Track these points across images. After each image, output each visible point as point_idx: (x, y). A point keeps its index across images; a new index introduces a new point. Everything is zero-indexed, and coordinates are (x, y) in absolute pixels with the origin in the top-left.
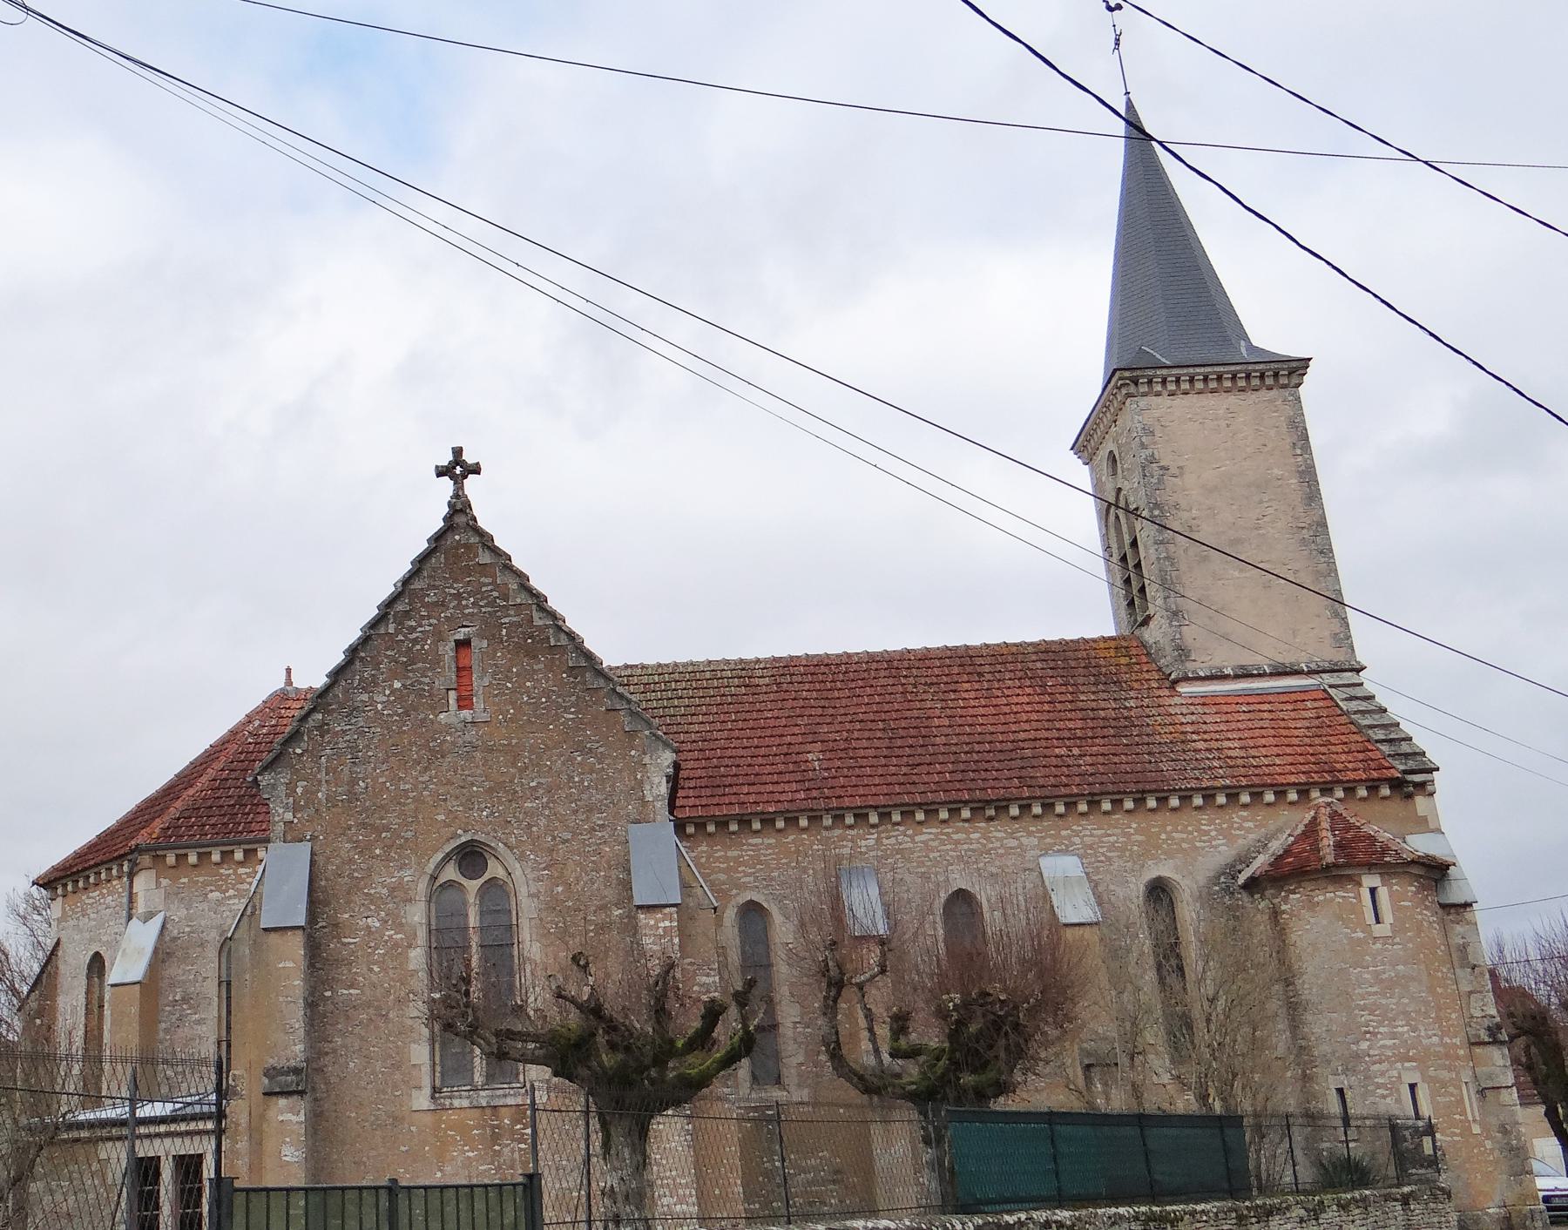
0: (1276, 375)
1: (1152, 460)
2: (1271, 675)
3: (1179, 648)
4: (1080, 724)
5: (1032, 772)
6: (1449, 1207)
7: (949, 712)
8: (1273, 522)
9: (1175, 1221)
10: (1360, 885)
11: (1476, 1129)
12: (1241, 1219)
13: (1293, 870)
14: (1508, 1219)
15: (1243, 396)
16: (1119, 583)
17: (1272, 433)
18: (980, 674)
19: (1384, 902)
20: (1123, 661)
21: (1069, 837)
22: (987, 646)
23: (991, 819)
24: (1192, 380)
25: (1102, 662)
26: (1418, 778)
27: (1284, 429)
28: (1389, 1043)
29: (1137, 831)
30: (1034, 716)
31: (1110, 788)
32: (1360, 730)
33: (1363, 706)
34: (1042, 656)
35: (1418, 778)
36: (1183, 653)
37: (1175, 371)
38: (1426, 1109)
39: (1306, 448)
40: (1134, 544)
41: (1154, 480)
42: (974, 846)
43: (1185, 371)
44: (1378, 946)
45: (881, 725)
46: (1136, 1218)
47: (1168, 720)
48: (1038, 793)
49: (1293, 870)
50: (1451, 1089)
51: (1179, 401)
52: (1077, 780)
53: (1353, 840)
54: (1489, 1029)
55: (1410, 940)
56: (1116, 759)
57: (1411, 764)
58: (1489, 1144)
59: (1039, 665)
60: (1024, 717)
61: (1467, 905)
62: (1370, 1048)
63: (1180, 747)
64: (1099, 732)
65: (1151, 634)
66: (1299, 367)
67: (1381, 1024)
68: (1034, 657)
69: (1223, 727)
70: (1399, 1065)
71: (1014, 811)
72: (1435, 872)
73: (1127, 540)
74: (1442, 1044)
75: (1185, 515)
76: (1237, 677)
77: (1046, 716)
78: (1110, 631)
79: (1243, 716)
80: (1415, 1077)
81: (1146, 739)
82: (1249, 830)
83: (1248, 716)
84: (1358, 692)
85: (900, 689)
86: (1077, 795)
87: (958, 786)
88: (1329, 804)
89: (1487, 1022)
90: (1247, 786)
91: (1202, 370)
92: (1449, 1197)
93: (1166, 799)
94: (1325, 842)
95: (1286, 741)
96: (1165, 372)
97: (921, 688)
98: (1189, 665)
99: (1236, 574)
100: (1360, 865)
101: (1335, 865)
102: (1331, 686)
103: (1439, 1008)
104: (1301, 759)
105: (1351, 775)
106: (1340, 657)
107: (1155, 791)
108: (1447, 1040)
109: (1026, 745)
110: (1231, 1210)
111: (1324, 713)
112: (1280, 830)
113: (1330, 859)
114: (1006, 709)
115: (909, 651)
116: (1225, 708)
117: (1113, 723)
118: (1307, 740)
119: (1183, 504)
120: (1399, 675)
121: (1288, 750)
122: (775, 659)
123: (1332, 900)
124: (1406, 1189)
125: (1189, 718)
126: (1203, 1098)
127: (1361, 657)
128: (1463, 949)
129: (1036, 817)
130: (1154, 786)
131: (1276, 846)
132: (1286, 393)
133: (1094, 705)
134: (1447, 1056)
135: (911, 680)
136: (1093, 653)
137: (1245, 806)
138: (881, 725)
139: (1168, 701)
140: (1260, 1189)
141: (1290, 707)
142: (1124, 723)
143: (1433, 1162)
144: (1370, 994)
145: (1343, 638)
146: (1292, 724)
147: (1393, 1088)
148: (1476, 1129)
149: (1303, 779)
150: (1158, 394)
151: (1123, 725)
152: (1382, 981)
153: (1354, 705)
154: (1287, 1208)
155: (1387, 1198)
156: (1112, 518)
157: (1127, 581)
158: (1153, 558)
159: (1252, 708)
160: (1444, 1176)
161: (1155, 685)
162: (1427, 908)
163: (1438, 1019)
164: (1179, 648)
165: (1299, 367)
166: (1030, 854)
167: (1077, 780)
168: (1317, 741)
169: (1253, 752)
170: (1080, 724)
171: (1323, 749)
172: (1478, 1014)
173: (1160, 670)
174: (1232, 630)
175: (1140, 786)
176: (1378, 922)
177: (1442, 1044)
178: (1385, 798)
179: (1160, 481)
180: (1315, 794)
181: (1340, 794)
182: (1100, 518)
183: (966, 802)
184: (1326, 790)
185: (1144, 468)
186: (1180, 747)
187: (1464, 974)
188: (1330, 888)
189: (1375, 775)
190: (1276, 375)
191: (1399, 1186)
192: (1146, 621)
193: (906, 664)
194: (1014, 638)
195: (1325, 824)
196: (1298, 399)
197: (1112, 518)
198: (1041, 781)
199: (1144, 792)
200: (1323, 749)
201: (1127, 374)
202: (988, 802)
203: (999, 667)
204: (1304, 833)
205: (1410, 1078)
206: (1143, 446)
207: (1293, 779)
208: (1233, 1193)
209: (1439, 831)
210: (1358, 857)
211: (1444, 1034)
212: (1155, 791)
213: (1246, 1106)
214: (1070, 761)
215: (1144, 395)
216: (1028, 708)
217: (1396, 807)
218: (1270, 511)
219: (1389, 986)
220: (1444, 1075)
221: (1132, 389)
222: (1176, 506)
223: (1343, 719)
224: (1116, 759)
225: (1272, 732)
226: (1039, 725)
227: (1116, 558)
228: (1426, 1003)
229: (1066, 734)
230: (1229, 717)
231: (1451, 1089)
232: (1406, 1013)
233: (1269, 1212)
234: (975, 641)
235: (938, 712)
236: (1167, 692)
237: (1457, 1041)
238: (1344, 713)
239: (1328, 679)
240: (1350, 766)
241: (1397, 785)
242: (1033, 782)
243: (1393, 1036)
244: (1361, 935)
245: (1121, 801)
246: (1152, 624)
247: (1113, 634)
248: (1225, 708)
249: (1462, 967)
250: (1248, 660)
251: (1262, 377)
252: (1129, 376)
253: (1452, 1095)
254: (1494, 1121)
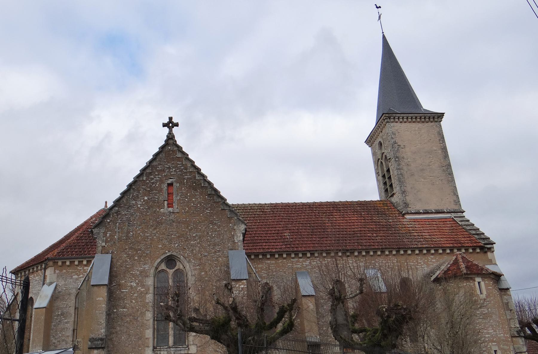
0: (434, 118)
2: (435, 213)
10: (475, 281)
13: (451, 275)
15: (423, 124)
18: (340, 210)
23: (348, 256)
24: (407, 118)
30: (360, 224)
31: (388, 246)
32: (467, 231)
36: (406, 205)
37: (402, 115)
39: (444, 141)
40: (388, 171)
41: (396, 149)
45: (309, 225)
48: (364, 248)
51: (403, 125)
52: (377, 244)
53: (471, 265)
54: (517, 332)
57: (486, 242)
59: (359, 208)
61: (508, 289)
65: (394, 200)
69: (421, 229)
72: (497, 277)
73: (385, 169)
74: (504, 337)
75: (406, 161)
76: (424, 213)
77: (363, 224)
79: (428, 226)
81: (397, 232)
82: (433, 262)
88: (460, 254)
89: (516, 329)
90: (434, 247)
94: (462, 266)
95: (443, 233)
96: (399, 115)
98: (409, 209)
100: (475, 274)
101: (467, 274)
105: (467, 245)
107: (403, 248)
109: (358, 232)
111: (454, 225)
112: (444, 263)
114: (350, 221)
116: (421, 223)
119: (405, 157)
122: (271, 204)
125: (410, 226)
127: (463, 208)
128: (507, 304)
132: (437, 123)
133: (378, 221)
137: (432, 254)
138: (309, 225)
139: (403, 220)
145: (457, 202)
146: (444, 228)
149: (451, 245)
150: (397, 122)
153: (463, 223)
157: (385, 184)
164: (405, 203)
167: (377, 244)
168: (453, 234)
169: (434, 237)
172: (513, 326)
173: (398, 210)
174: (421, 198)
175: (398, 246)
178: (478, 253)
179: (398, 149)
180: (455, 251)
181: (463, 251)
183: (340, 250)
184: (459, 250)
187: (508, 312)
188: (465, 282)
189: (475, 245)
190: (434, 118)
193: (315, 207)
195: (461, 260)
197: (379, 163)
198: (365, 244)
199: (399, 248)
201: (387, 115)
202: (348, 250)
204: (453, 263)
205: (494, 348)
206: (392, 138)
207: (448, 245)
209: (496, 264)
210: (475, 271)
212: (403, 248)
215: (392, 122)
216: (357, 221)
217: (481, 256)
221: (389, 120)
222: (403, 158)
223: (460, 227)
229: (371, 229)
232: (492, 326)
235: (327, 222)
237: (508, 335)
238: (461, 225)
241: (482, 248)
248: (421, 223)
251: (429, 118)
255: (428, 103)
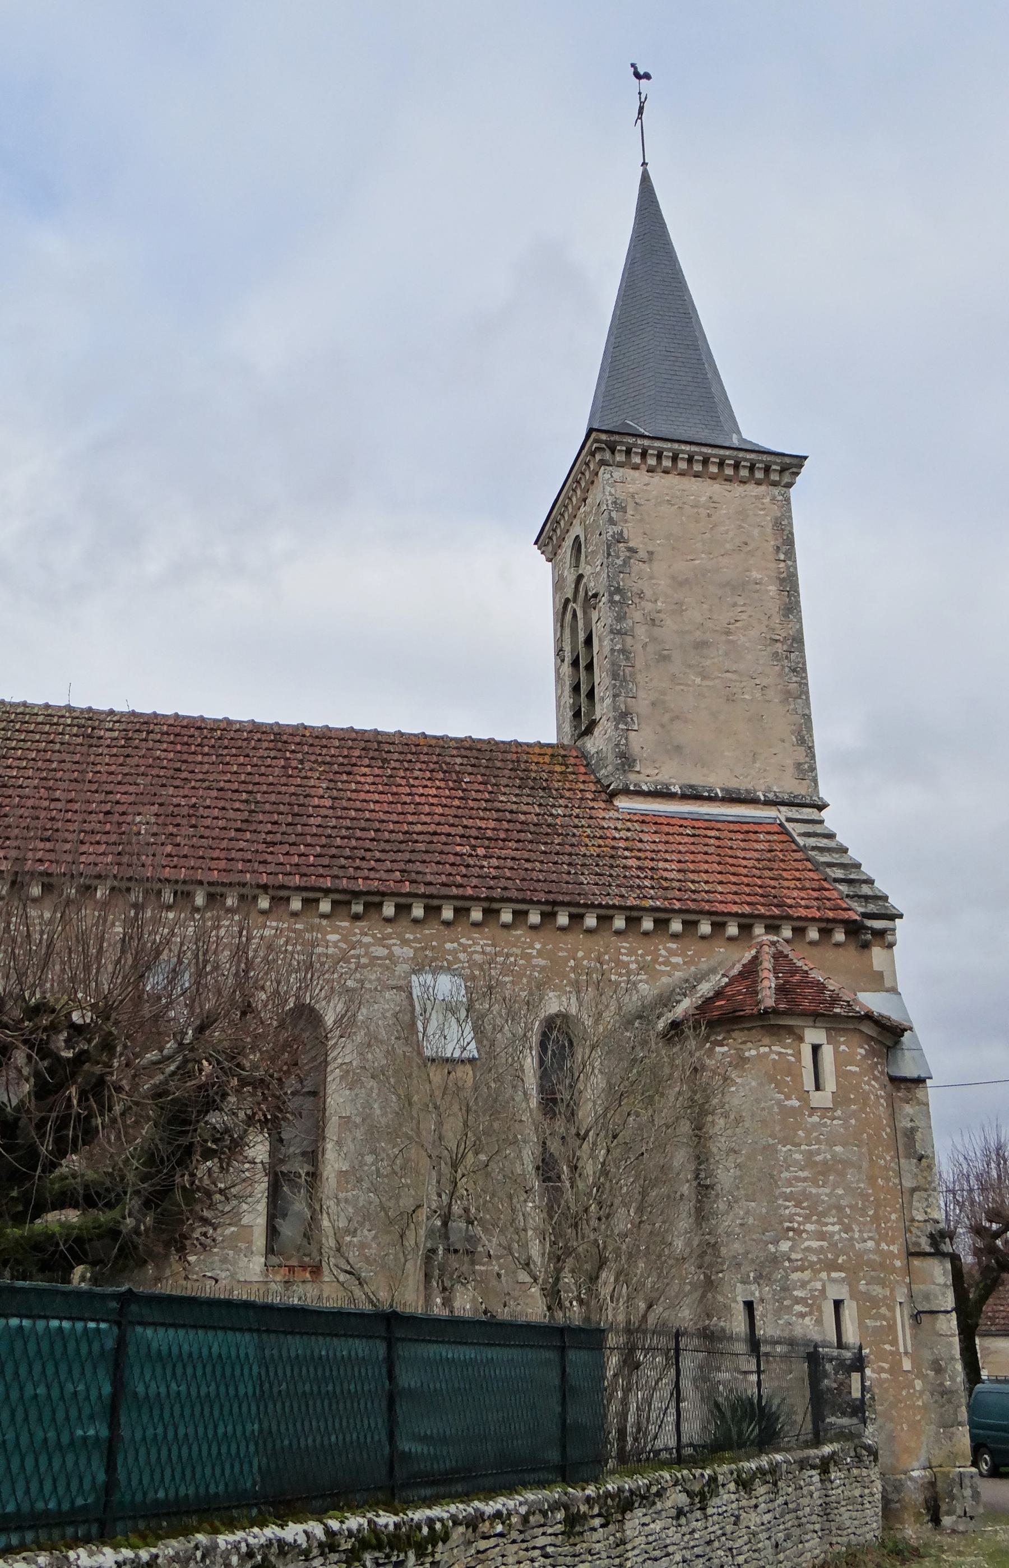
0: (767, 470)
1: (620, 538)
2: (723, 800)
3: (622, 755)
4: (492, 824)
5: (419, 867)
6: (874, 1473)
7: (335, 793)
8: (745, 628)
9: (438, 1537)
10: (801, 1039)
11: (907, 1365)
12: (574, 1522)
13: (726, 1016)
14: (933, 1484)
15: (728, 486)
16: (567, 689)
17: (756, 532)
18: (384, 760)
19: (831, 1058)
20: (558, 768)
21: (454, 952)
22: (401, 734)
23: (356, 917)
24: (675, 458)
25: (533, 767)
26: (878, 924)
27: (769, 530)
28: (815, 1244)
29: (540, 953)
30: (439, 810)
31: (514, 894)
32: (817, 867)
33: (824, 842)
34: (463, 752)
35: (878, 924)
36: (626, 761)
37: (657, 444)
38: (851, 1335)
39: (790, 554)
40: (589, 641)
41: (619, 562)
42: (330, 951)
43: (669, 445)
44: (815, 1119)
45: (244, 796)
46: (330, 1545)
47: (599, 833)
48: (422, 889)
49: (726, 1016)
50: (883, 1310)
51: (658, 480)
52: (474, 881)
53: (799, 984)
54: (931, 1236)
55: (854, 1114)
56: (528, 865)
57: (871, 908)
58: (918, 1384)
59: (459, 760)
60: (427, 809)
61: (920, 1081)
62: (792, 1249)
63: (608, 861)
64: (515, 835)
65: (593, 744)
66: (790, 466)
67: (807, 1218)
68: (455, 752)
69: (661, 847)
70: (824, 1275)
71: (389, 910)
72: (888, 1035)
73: (582, 636)
74: (878, 1251)
75: (649, 606)
76: (684, 797)
77: (453, 811)
78: (550, 737)
79: (686, 839)
80: (841, 1292)
81: (568, 849)
82: (675, 967)
83: (692, 840)
84: (818, 829)
85: (282, 762)
86: (471, 898)
87: (321, 871)
88: (773, 943)
89: (929, 1228)
90: (680, 911)
91: (687, 448)
92: (876, 1460)
93: (582, 917)
94: (766, 983)
95: (732, 869)
96: (646, 442)
97: (307, 765)
98: (633, 777)
99: (698, 680)
100: (804, 1014)
101: (775, 1012)
102: (789, 820)
103: (878, 1205)
104: (747, 890)
105: (803, 912)
106: (801, 789)
107: (568, 904)
108: (884, 1246)
109: (421, 838)
110: (555, 1506)
111: (778, 847)
112: (713, 971)
113: (770, 1002)
114: (408, 799)
115: (306, 728)
116: (666, 829)
117: (532, 828)
118: (757, 872)
119: (648, 593)
120: (862, 818)
121: (733, 879)
122: (133, 713)
123: (766, 1055)
124: (827, 1449)
125: (624, 834)
126: (553, 1295)
127: (824, 793)
128: (910, 1134)
129: (416, 921)
130: (567, 899)
131: (705, 988)
132: (776, 491)
133: (514, 807)
134: (882, 1266)
135: (300, 756)
136: (525, 757)
137: (675, 936)
138: (244, 796)
139: (601, 814)
140: (622, 1457)
141: (741, 836)
142: (545, 829)
143: (858, 1409)
144: (798, 1179)
145: (807, 770)
146: (740, 854)
147: (813, 1306)
148: (907, 1365)
149: (747, 909)
150: (636, 467)
151: (544, 830)
152: (816, 1163)
153: (812, 841)
154: (659, 1494)
155: (803, 1464)
156: (569, 616)
157: (576, 689)
158: (606, 650)
159: (697, 832)
160: (870, 1429)
161: (590, 796)
162: (875, 1079)
163: (876, 1218)
164: (622, 755)
165: (790, 466)
166: (402, 969)
167: (474, 881)
168: (767, 873)
169: (692, 876)
170: (492, 824)
171: (773, 883)
172: (920, 1217)
173: (598, 781)
174: (685, 747)
175: (551, 897)
176: (818, 1088)
177: (878, 1251)
178: (838, 945)
179: (626, 562)
180: (759, 930)
181: (787, 933)
182: (555, 614)
183: (327, 891)
184: (772, 928)
185: (609, 547)
186: (608, 861)
187: (908, 1165)
188: (766, 1040)
189: (831, 914)
190: (767, 470)
191: (817, 1441)
192: (589, 731)
193: (297, 739)
194: (434, 730)
195: (767, 963)
196: (788, 500)
197: (569, 616)
198: (429, 878)
199: (554, 903)
200: (773, 883)
201: (604, 437)
202: (356, 894)
203: (410, 757)
204: (740, 973)
205: (835, 1292)
206: (612, 521)
207: (735, 909)
208: (567, 1473)
209: (894, 990)
210: (801, 1005)
211: (883, 1237)
212: (568, 904)
213: (614, 1314)
214: (471, 861)
215: (621, 465)
216: (435, 801)
217: (850, 956)
218: (744, 616)
219: (823, 1171)
220: (877, 1291)
221: (607, 455)
222: (641, 595)
223: (798, 855)
224: (528, 865)
225: (718, 859)
226: (443, 820)
227: (568, 660)
228: (864, 1197)
229: (474, 832)
230: (671, 839)
231: (883, 1310)
232: (840, 1209)
233: (626, 1503)
234: (388, 726)
235: (321, 792)
236: (603, 805)
237: (894, 1249)
238: (800, 849)
239: (785, 812)
240: (803, 903)
241: (854, 929)
242: (419, 878)
243: (821, 1236)
244: (796, 1103)
245: (526, 913)
246: (597, 731)
247: (554, 741)
248: (666, 829)
249: (908, 1157)
250: (698, 778)
251: (752, 468)
252: (606, 443)
253: (884, 1318)
254: (927, 1355)
255: (758, 422)
